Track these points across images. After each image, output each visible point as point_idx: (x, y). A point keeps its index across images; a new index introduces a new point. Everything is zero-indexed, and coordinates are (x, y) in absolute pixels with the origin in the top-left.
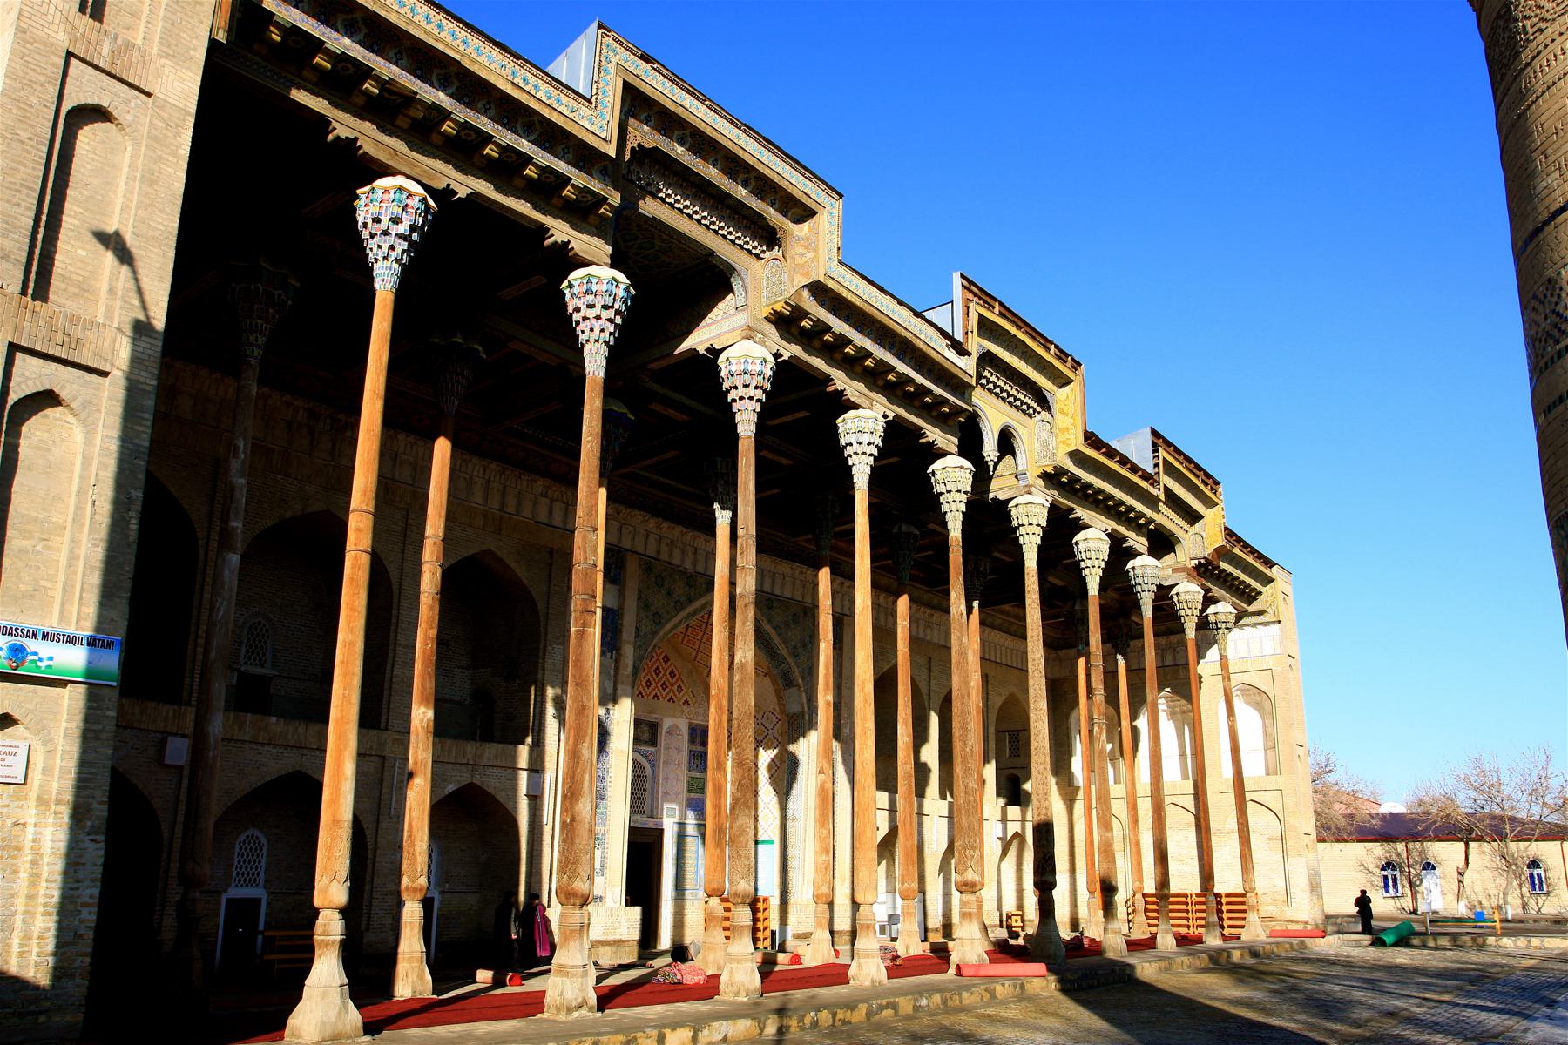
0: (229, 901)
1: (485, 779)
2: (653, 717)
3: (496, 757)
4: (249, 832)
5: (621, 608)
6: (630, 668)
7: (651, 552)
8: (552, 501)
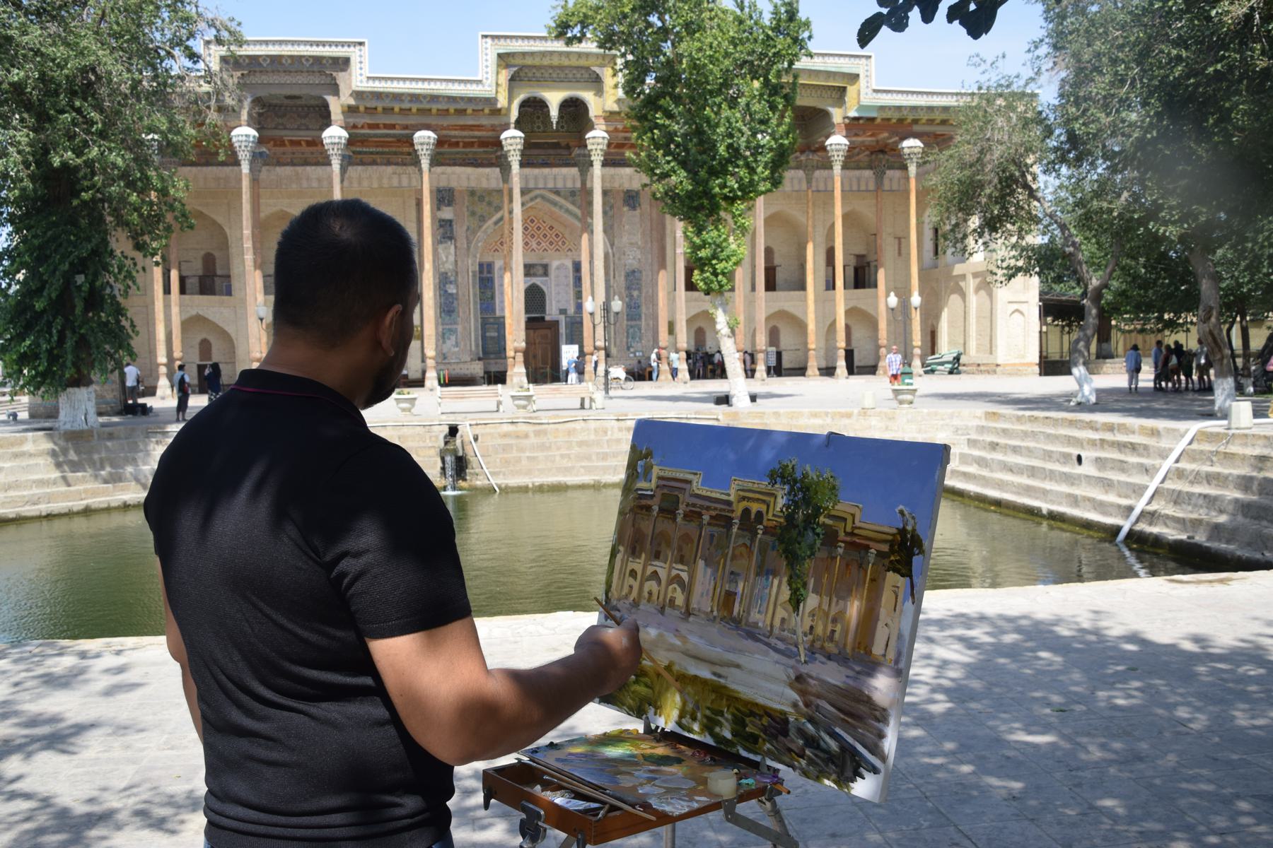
2: (545, 261)
7: (473, 184)
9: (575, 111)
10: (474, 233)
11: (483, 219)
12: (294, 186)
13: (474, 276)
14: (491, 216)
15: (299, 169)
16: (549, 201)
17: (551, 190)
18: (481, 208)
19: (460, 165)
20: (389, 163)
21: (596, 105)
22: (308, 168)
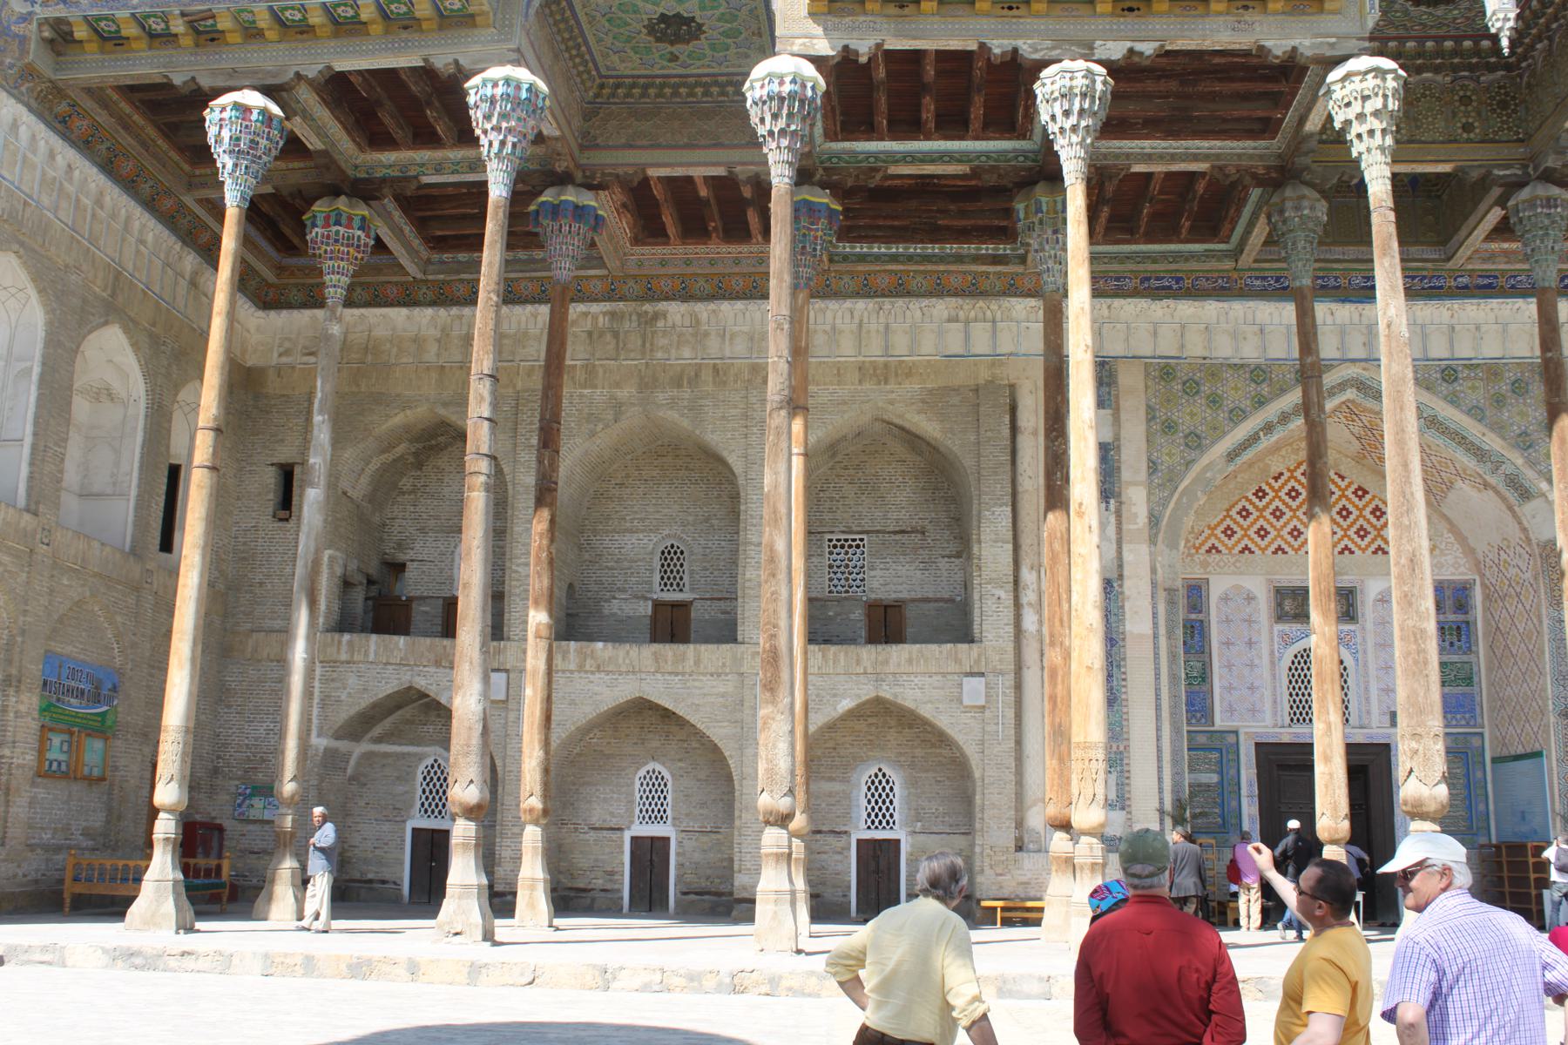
0: (634, 839)
1: (898, 690)
2: (1346, 581)
3: (910, 661)
4: (650, 767)
5: (1117, 438)
6: (1142, 519)
7: (1167, 347)
8: (967, 322)
10: (1172, 480)
11: (1196, 442)
12: (687, 352)
13: (1171, 603)
14: (1218, 433)
15: (703, 309)
18: (1192, 413)
19: (1135, 293)
20: (939, 290)
22: (726, 307)
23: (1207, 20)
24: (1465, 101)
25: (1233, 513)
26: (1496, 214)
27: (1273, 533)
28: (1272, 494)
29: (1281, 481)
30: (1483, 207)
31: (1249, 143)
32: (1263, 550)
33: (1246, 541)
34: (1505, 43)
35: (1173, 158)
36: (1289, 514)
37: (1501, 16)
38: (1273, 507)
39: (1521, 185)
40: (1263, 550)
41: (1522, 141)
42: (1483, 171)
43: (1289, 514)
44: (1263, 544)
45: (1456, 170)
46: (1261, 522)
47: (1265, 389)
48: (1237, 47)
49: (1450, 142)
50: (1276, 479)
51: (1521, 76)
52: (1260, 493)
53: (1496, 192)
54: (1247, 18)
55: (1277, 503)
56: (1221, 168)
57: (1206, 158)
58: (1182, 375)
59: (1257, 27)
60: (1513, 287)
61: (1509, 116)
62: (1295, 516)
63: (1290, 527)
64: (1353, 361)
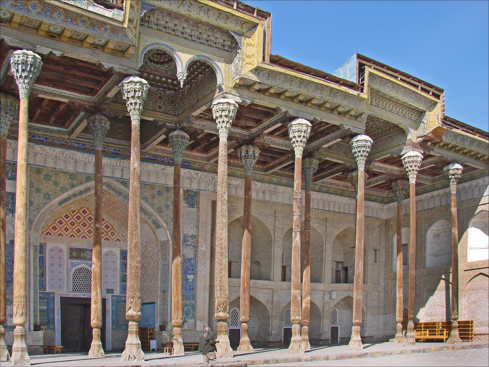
9: (202, 73)
16: (114, 190)
17: (117, 179)
21: (226, 74)
23: (82, 49)
24: (160, 98)
25: (57, 222)
26: (164, 137)
27: (70, 230)
28: (71, 217)
29: (74, 213)
30: (159, 134)
31: (84, 96)
32: (67, 235)
33: (61, 232)
34: (182, 84)
35: (55, 95)
36: (76, 224)
37: (182, 75)
38: (71, 221)
39: (174, 130)
40: (67, 235)
41: (176, 115)
42: (163, 123)
43: (76, 224)
44: (67, 233)
45: (155, 120)
46: (66, 226)
47: (75, 182)
48: (91, 61)
49: (153, 111)
50: (73, 212)
51: (179, 94)
52: (67, 216)
53: (164, 130)
54: (96, 52)
55: (72, 220)
56: (73, 103)
57: (67, 97)
58: (44, 173)
59: (100, 55)
60: (162, 161)
61: (173, 106)
62: (78, 225)
63: (77, 228)
64: (107, 177)
